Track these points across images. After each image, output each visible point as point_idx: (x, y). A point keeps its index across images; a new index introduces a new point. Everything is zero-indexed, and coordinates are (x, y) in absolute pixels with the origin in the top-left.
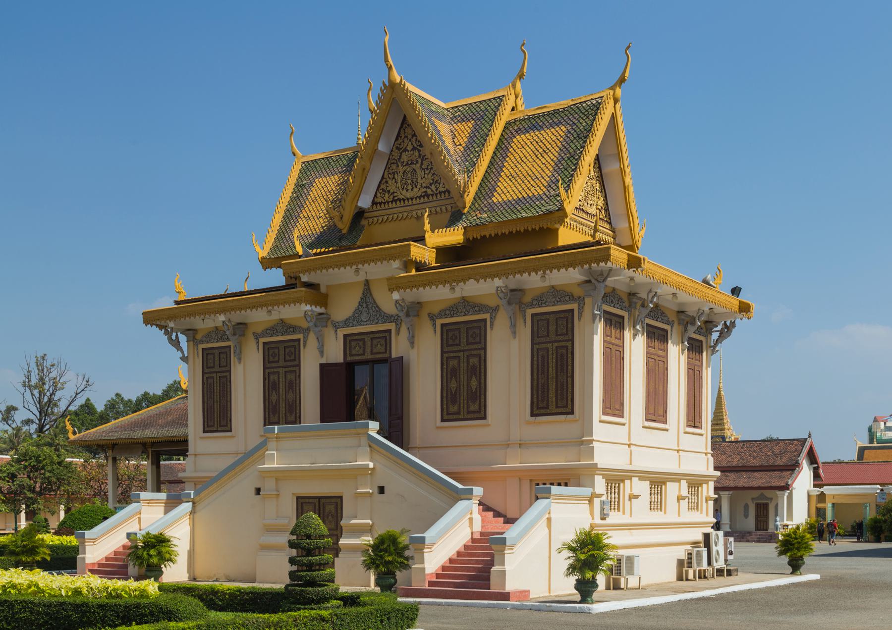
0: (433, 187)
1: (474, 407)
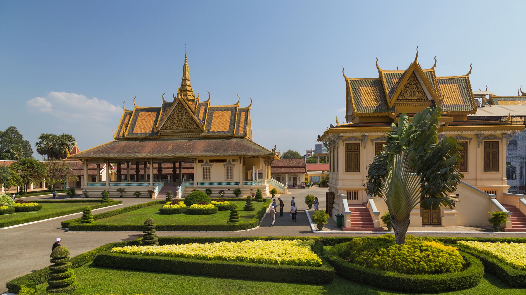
0: (422, 97)
1: (463, 168)
